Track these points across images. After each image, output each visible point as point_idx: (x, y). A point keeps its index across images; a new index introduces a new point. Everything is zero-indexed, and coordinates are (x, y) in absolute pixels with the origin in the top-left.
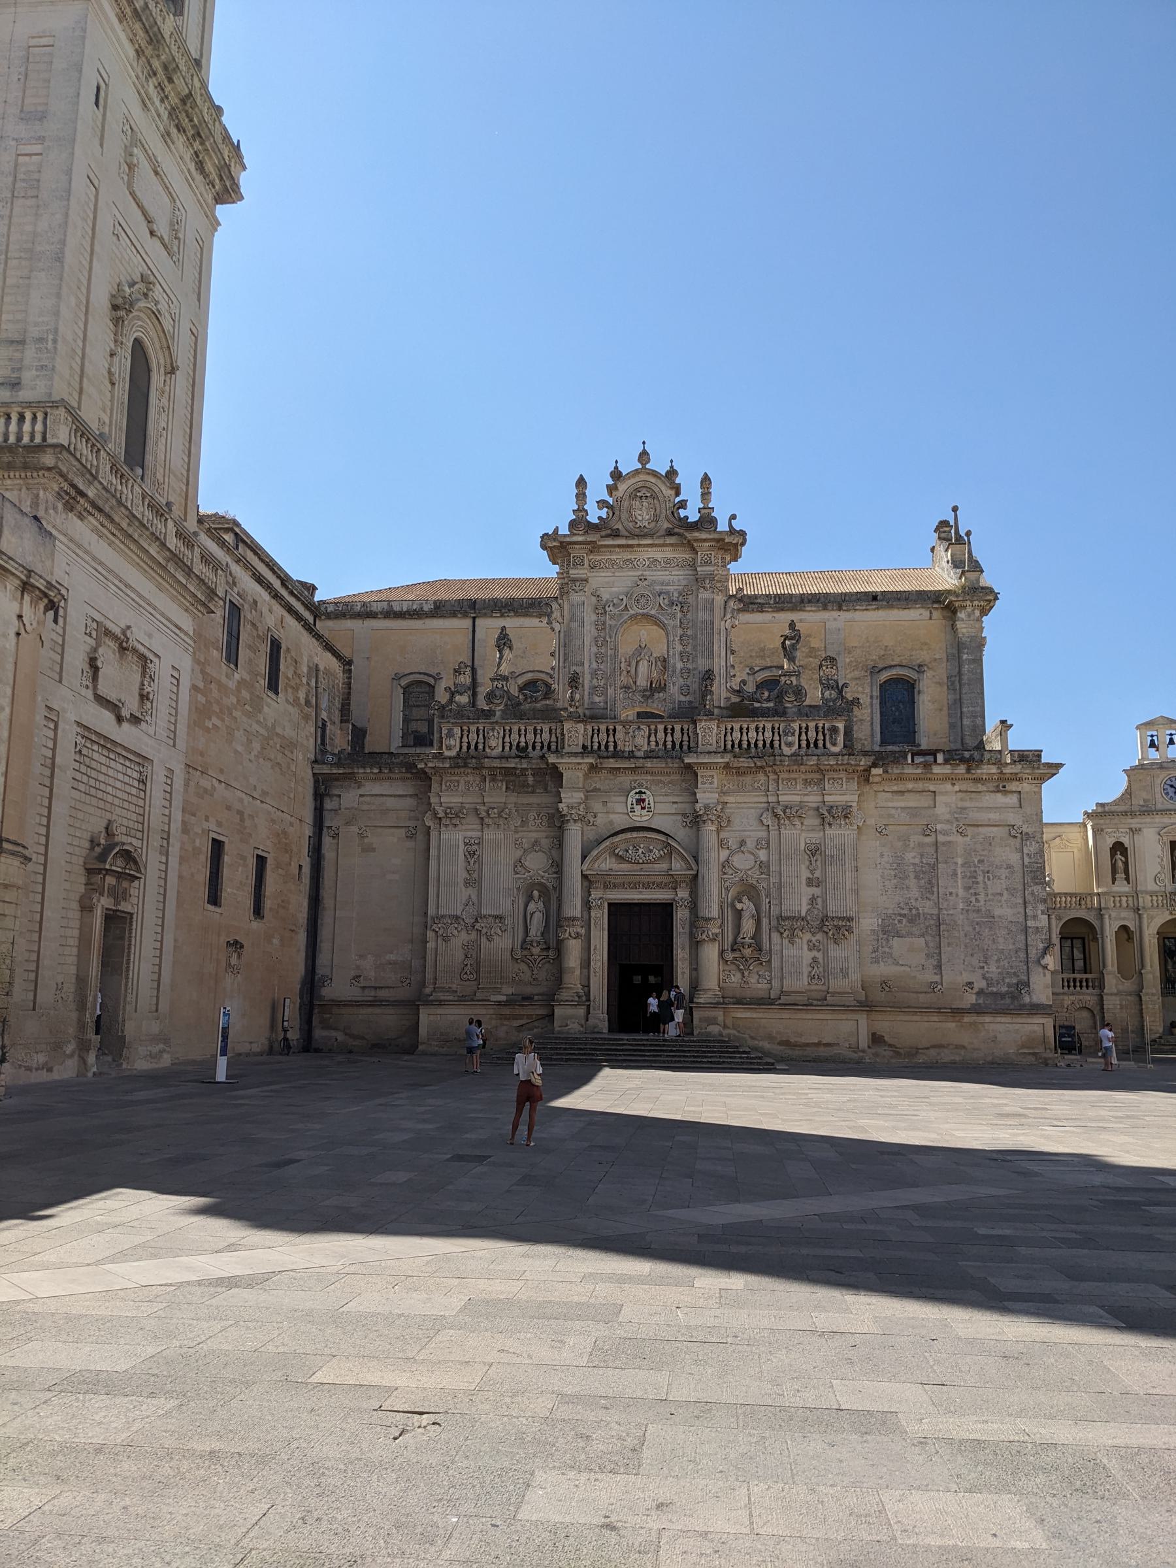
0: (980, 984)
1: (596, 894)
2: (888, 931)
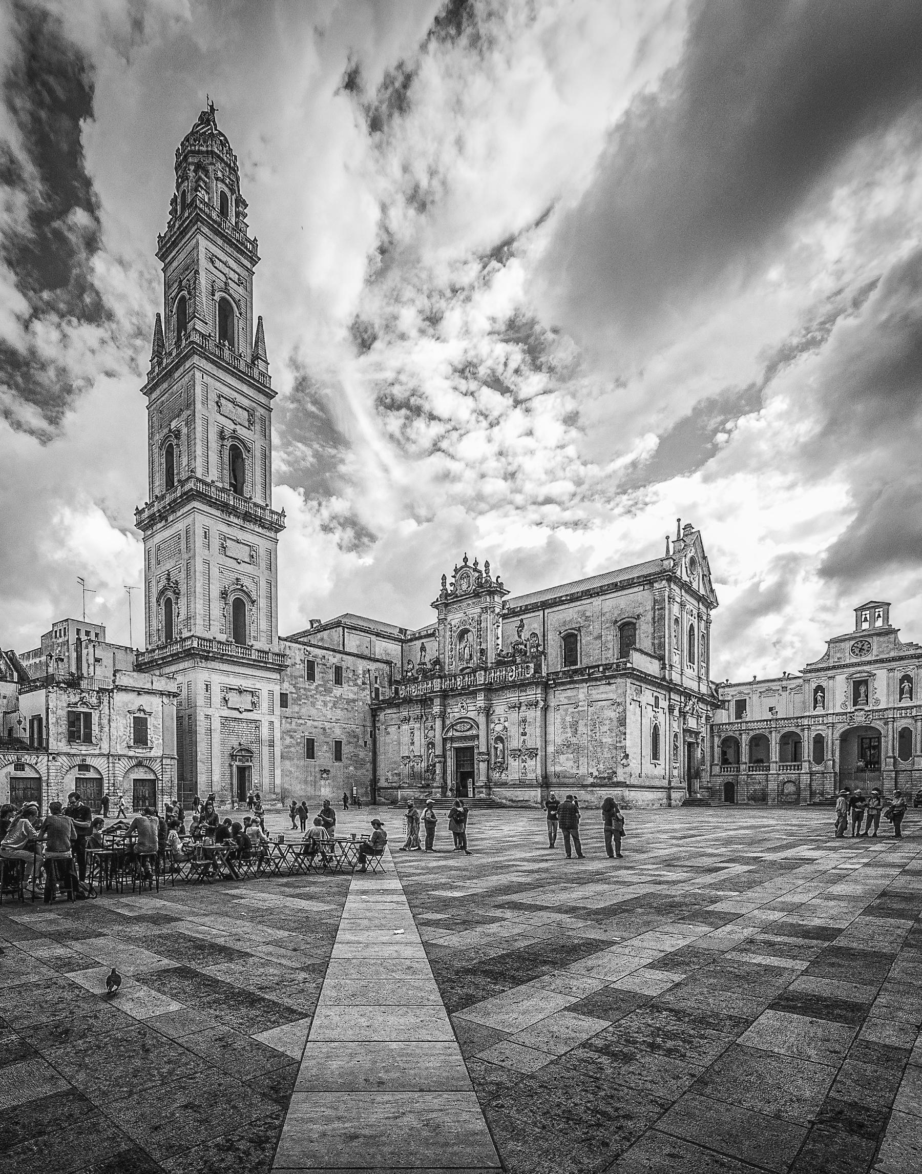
0: (596, 773)
1: (449, 745)
2: (558, 752)
